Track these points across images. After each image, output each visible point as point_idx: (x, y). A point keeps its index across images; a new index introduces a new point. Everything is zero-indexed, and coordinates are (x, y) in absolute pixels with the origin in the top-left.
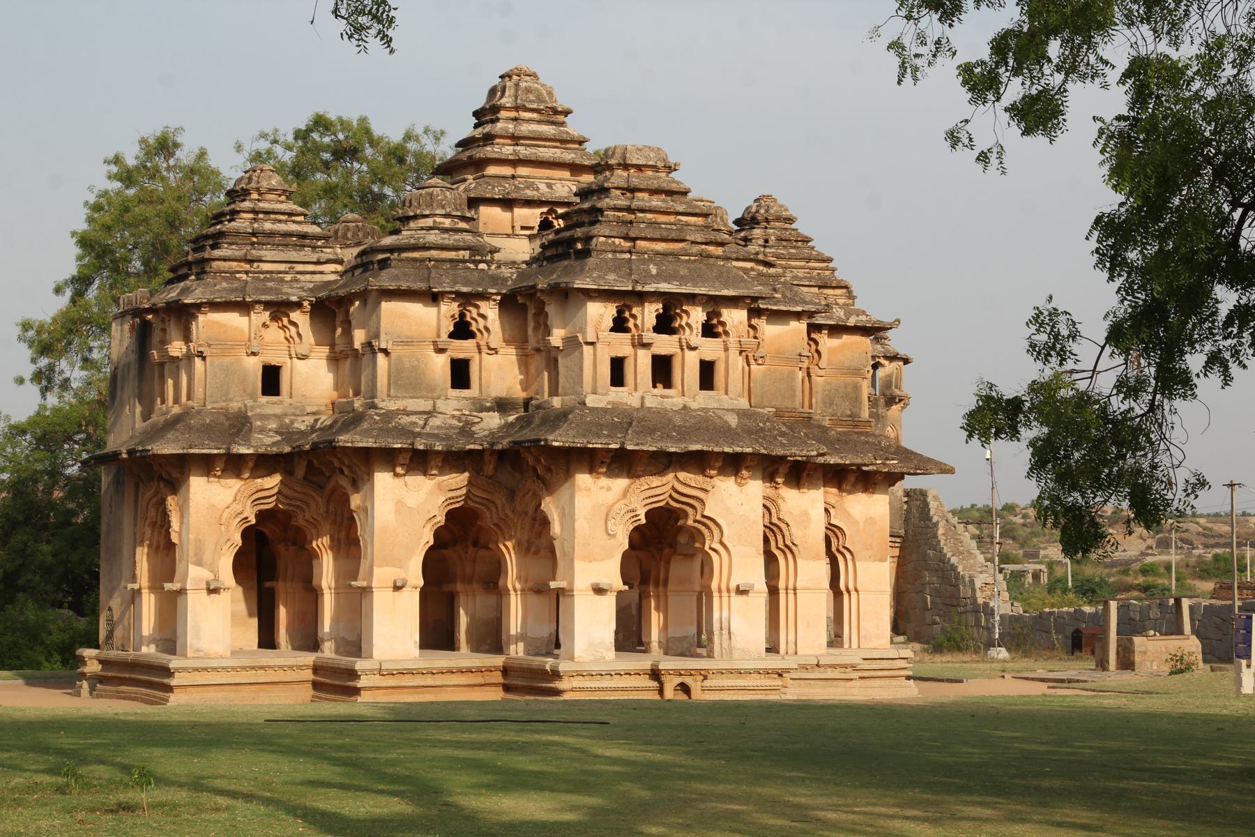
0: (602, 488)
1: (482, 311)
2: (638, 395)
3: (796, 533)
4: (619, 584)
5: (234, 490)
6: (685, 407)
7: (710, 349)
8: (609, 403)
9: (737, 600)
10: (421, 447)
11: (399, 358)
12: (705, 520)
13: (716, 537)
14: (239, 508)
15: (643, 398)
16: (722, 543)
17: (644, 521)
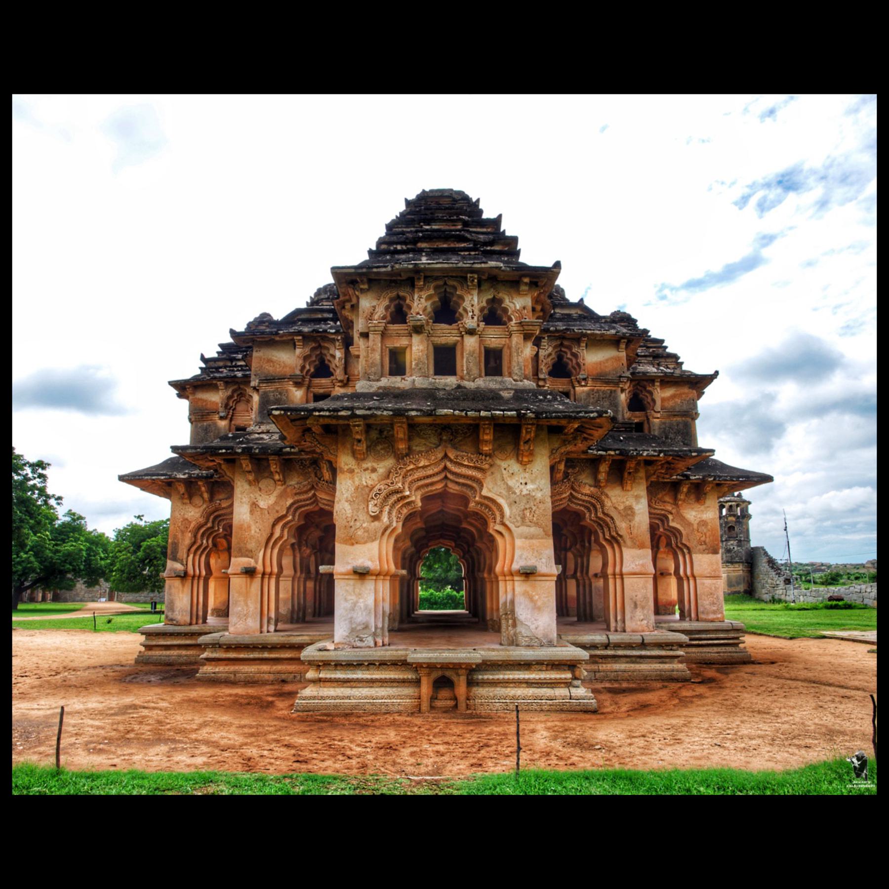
0: (367, 469)
1: (331, 352)
2: (410, 379)
3: (622, 526)
4: (393, 568)
5: (202, 509)
6: (459, 387)
7: (494, 337)
8: (380, 388)
9: (520, 586)
10: (240, 451)
11: (265, 393)
12: (486, 502)
13: (498, 519)
14: (202, 520)
15: (414, 381)
16: (503, 524)
17: (420, 504)
